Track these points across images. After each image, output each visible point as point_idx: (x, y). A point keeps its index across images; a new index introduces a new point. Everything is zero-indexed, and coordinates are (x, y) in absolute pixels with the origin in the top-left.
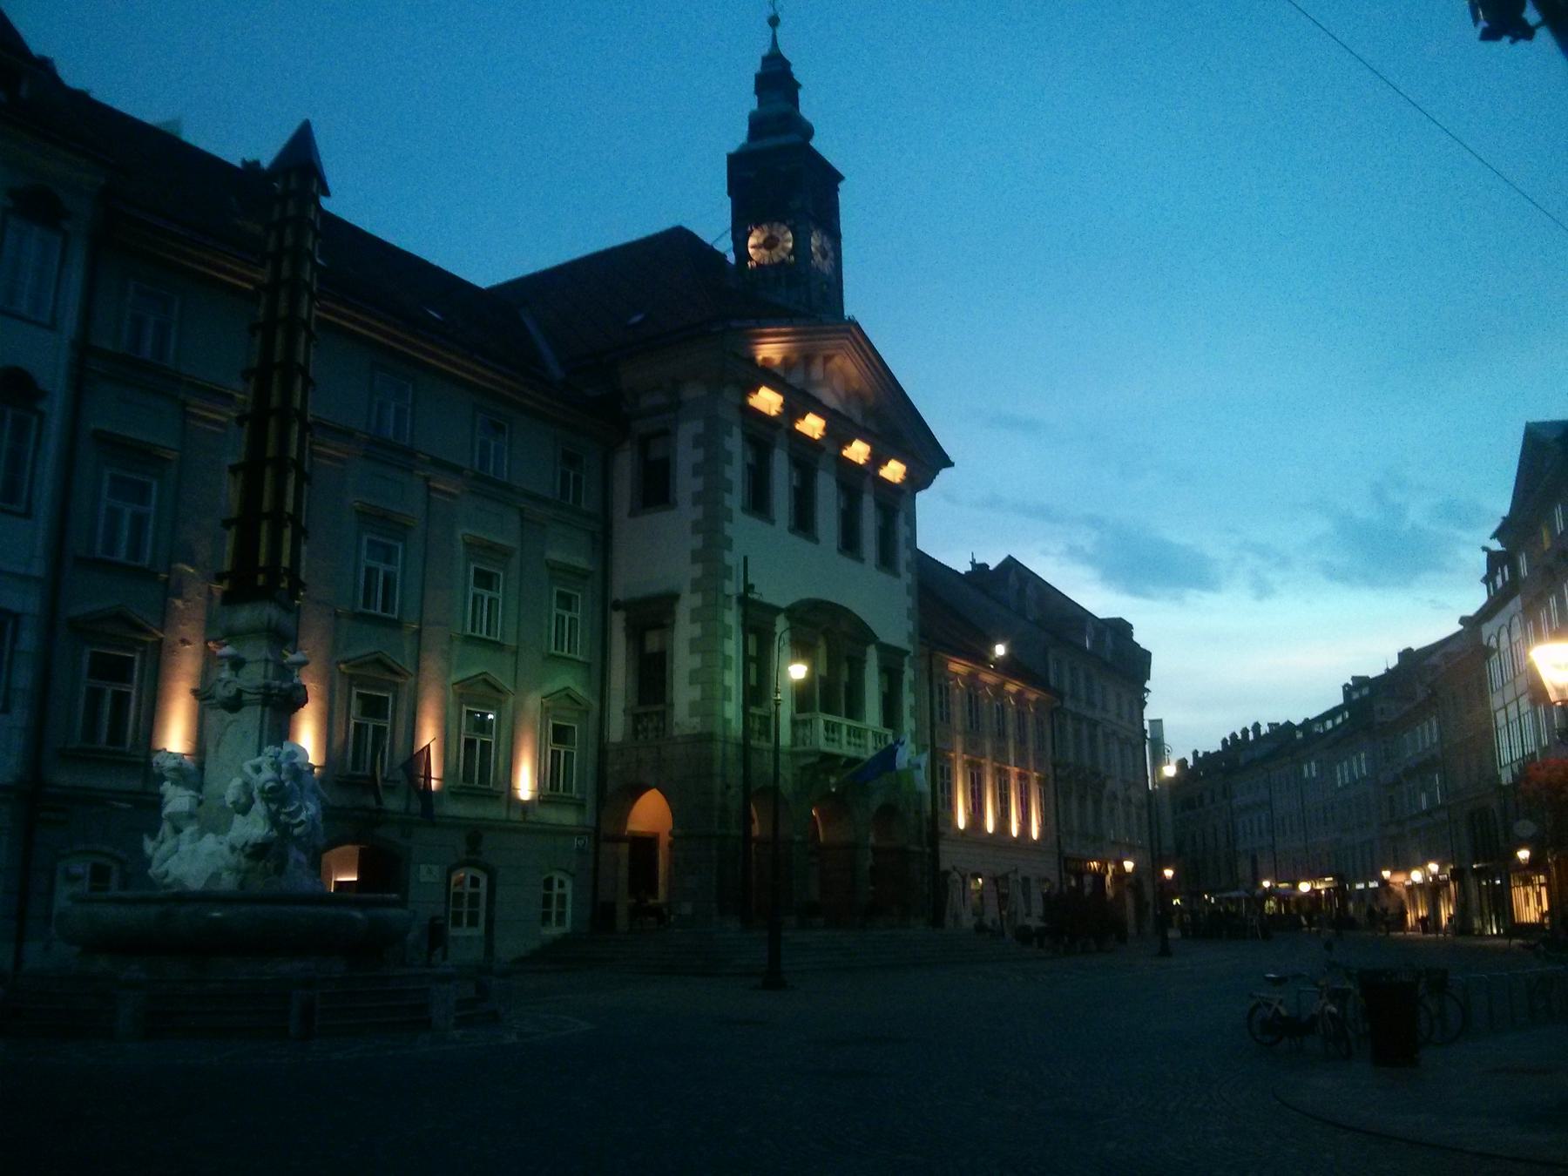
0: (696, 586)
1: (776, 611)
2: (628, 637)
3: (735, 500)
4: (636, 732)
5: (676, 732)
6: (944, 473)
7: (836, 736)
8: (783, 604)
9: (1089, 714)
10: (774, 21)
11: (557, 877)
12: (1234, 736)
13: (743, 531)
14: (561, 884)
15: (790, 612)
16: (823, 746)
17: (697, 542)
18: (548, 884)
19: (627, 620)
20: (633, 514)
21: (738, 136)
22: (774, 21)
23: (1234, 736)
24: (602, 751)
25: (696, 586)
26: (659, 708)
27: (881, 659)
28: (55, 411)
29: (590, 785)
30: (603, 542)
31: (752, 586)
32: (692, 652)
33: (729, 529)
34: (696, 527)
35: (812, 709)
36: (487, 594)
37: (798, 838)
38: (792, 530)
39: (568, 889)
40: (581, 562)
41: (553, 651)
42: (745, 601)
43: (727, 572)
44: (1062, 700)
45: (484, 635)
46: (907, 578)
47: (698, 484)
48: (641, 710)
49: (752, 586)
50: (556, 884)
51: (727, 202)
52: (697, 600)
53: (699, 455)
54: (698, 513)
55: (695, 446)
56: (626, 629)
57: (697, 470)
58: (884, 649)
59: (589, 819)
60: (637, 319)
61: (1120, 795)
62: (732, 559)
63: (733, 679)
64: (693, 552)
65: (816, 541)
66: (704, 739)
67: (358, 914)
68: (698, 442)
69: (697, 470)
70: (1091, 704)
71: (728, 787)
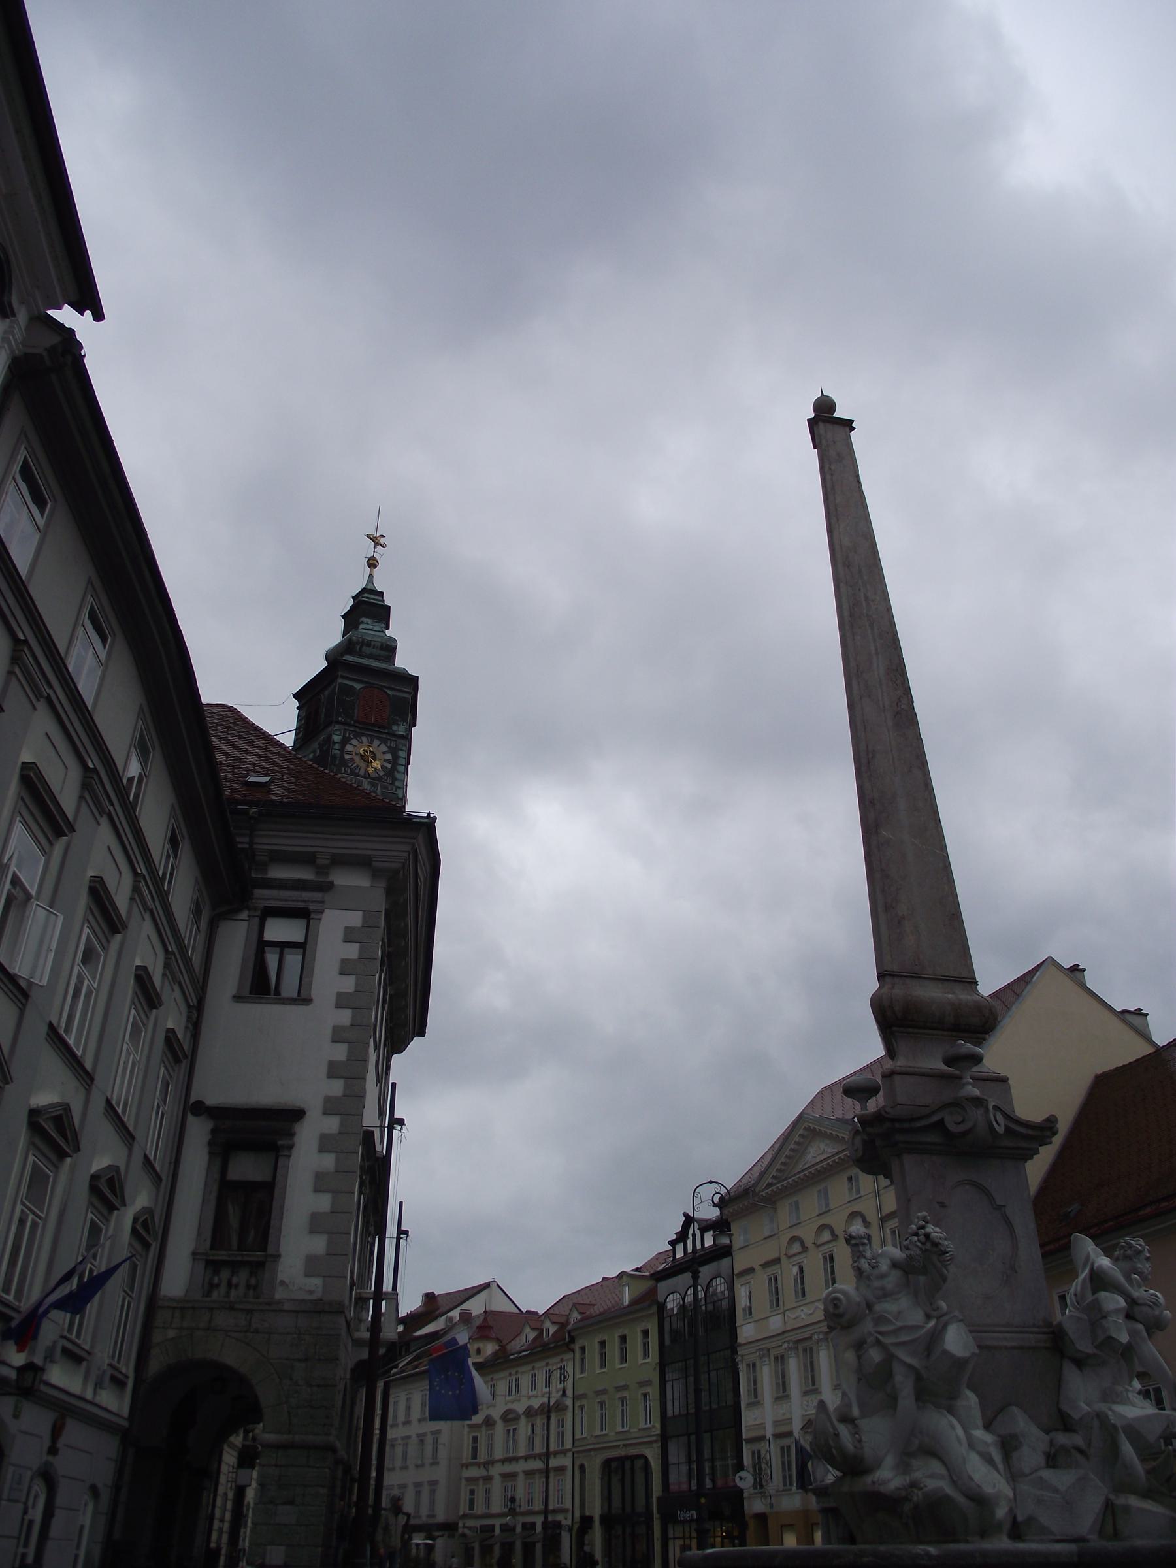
5: (279, 1294)
10: (372, 563)
17: (340, 1052)
19: (214, 1132)
20: (238, 998)
22: (372, 563)
25: (330, 1107)
34: (338, 1035)
48: (222, 1255)
52: (332, 1124)
54: (345, 1017)
55: (347, 940)
56: (211, 1144)
57: (346, 968)
64: (331, 1064)
68: (349, 935)
69: (346, 968)
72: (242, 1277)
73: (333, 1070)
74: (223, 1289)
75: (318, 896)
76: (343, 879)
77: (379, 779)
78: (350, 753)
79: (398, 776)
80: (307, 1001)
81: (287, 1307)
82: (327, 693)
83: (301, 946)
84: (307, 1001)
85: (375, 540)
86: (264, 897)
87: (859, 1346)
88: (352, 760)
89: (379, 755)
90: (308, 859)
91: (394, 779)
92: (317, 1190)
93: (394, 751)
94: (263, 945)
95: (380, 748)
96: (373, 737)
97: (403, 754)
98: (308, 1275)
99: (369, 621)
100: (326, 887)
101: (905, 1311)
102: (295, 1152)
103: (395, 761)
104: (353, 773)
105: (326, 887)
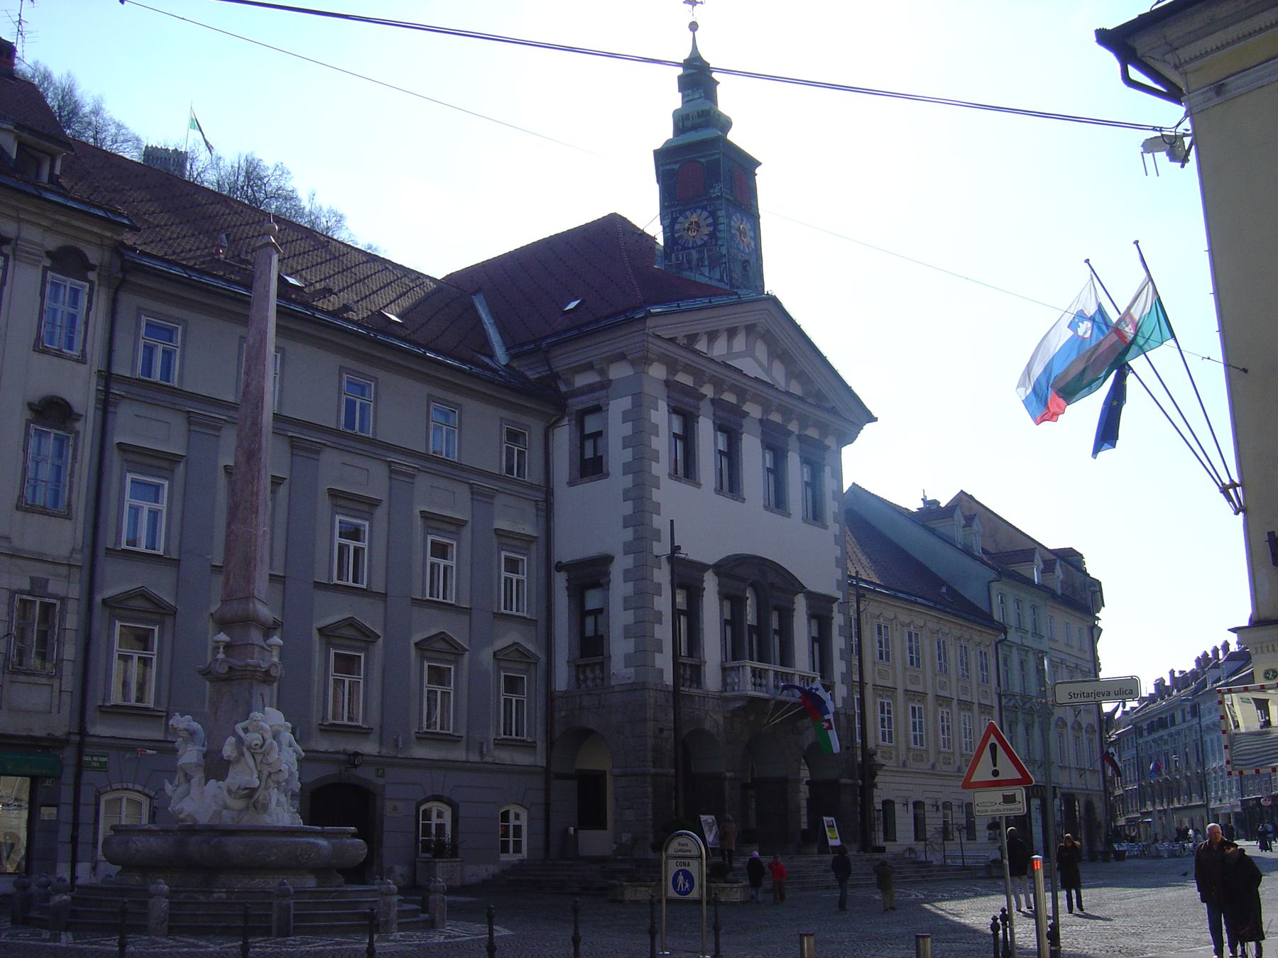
1: (703, 567)
3: (661, 468)
4: (578, 679)
6: (868, 428)
7: (764, 682)
8: (711, 562)
9: (1036, 645)
10: (694, 27)
11: (513, 810)
12: (1205, 654)
13: (672, 498)
14: (517, 817)
15: (719, 568)
16: (751, 691)
18: (505, 816)
21: (664, 133)
22: (694, 27)
23: (1205, 654)
24: (550, 697)
25: (628, 549)
26: (599, 659)
27: (809, 607)
28: (87, 429)
29: (540, 729)
30: (546, 509)
31: (679, 548)
33: (656, 495)
34: (627, 495)
35: (743, 658)
36: (442, 562)
37: (728, 775)
38: (719, 490)
39: (524, 821)
40: (529, 530)
41: (503, 610)
42: (672, 559)
43: (657, 535)
44: (1005, 632)
45: (441, 599)
46: (834, 528)
47: (628, 455)
48: (582, 662)
49: (679, 548)
50: (512, 816)
51: (657, 187)
52: (629, 561)
53: (627, 429)
54: (628, 481)
58: (811, 596)
59: (541, 761)
60: (572, 305)
61: (1070, 722)
62: (660, 522)
63: (664, 632)
65: (743, 500)
66: (638, 687)
67: (322, 842)
68: (626, 417)
70: (1037, 634)
71: (661, 730)
73: (627, 522)
76: (618, 372)
77: (705, 244)
84: (607, 475)
86: (576, 404)
89: (702, 223)
90: (589, 367)
91: (717, 239)
93: (713, 214)
97: (720, 213)
100: (605, 385)
103: (715, 224)
104: (684, 248)
105: (605, 385)
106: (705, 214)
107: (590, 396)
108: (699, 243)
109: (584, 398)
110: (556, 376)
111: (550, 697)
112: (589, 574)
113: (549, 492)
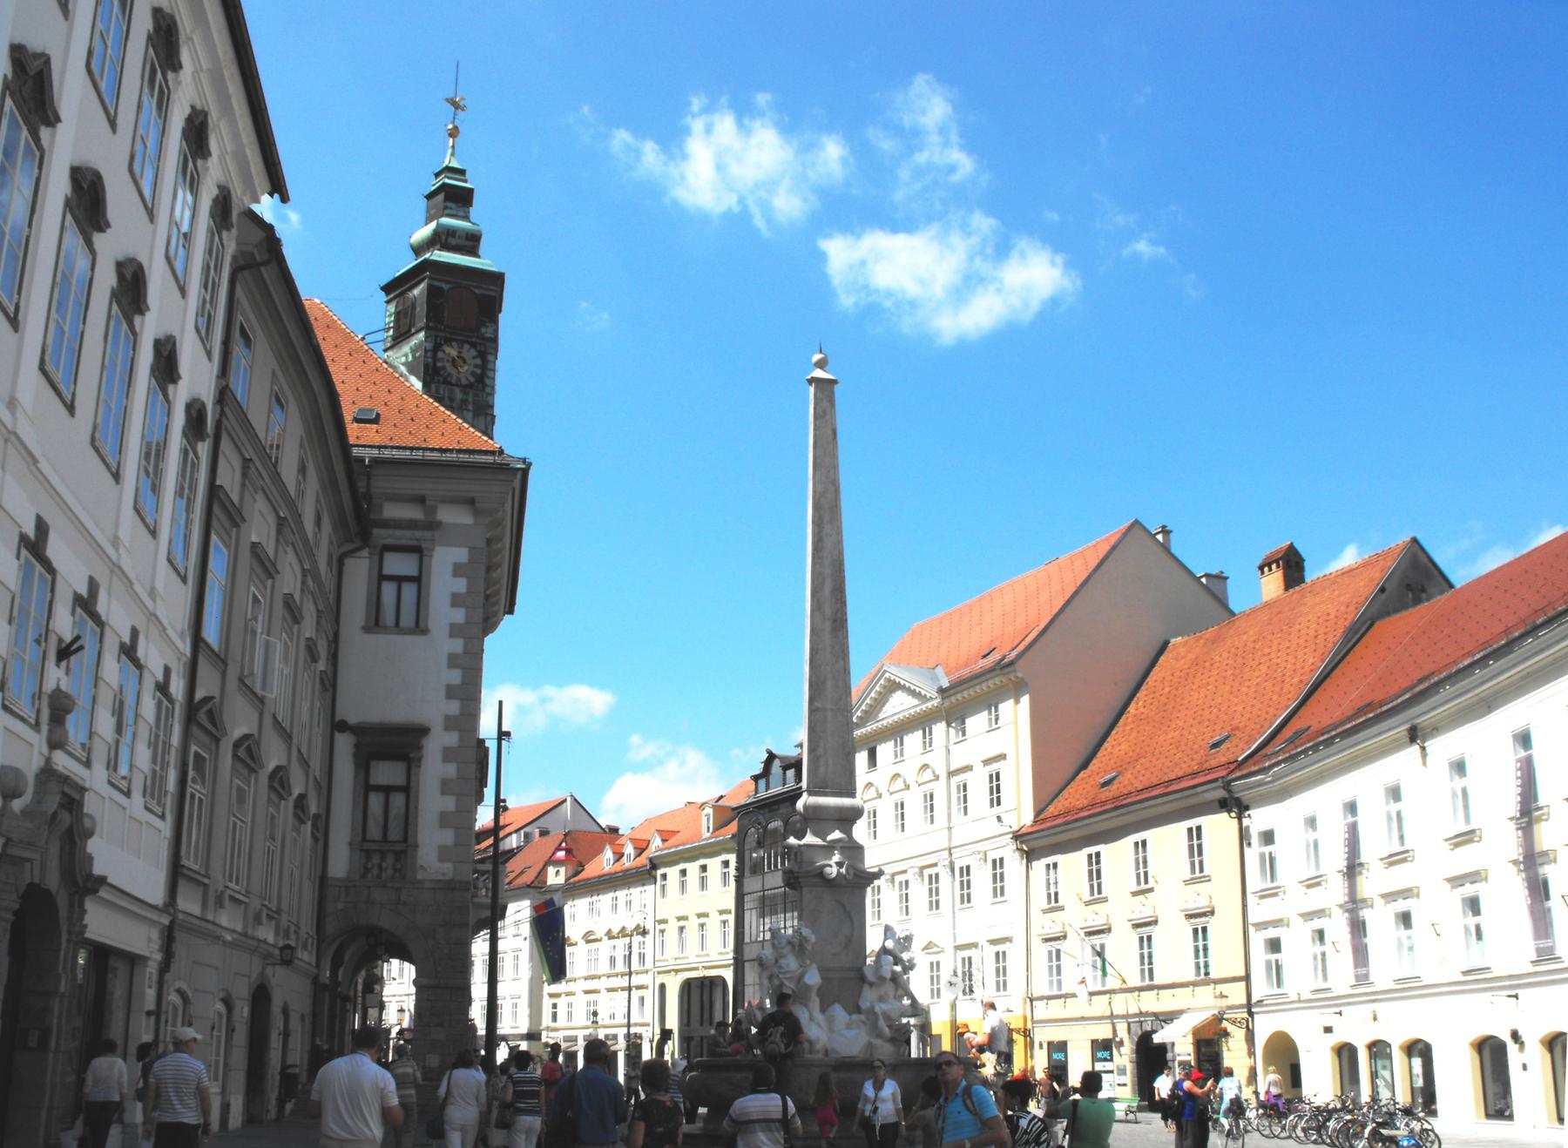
0: (450, 723)
2: (357, 765)
5: (419, 877)
17: (455, 677)
19: (357, 746)
20: (367, 629)
24: (323, 881)
25: (450, 723)
32: (443, 793)
49: (508, 734)
52: (452, 739)
54: (457, 645)
56: (355, 756)
57: (456, 601)
68: (458, 570)
69: (456, 601)
72: (390, 859)
73: (451, 692)
74: (375, 871)
75: (428, 534)
76: (452, 516)
77: (470, 386)
78: (442, 360)
79: (488, 381)
80: (425, 632)
81: (427, 885)
82: (416, 292)
83: (417, 580)
84: (425, 632)
85: (456, 105)
86: (382, 536)
87: (770, 978)
88: (444, 368)
90: (421, 500)
91: (485, 386)
92: (443, 793)
94: (383, 578)
95: (470, 353)
96: (463, 342)
98: (441, 860)
99: (452, 205)
101: (791, 963)
102: (424, 761)
104: (446, 382)
105: (433, 526)
106: (473, 352)
107: (408, 533)
108: (464, 382)
109: (398, 533)
110: (368, 496)
111: (323, 881)
112: (395, 744)
113: (336, 635)
